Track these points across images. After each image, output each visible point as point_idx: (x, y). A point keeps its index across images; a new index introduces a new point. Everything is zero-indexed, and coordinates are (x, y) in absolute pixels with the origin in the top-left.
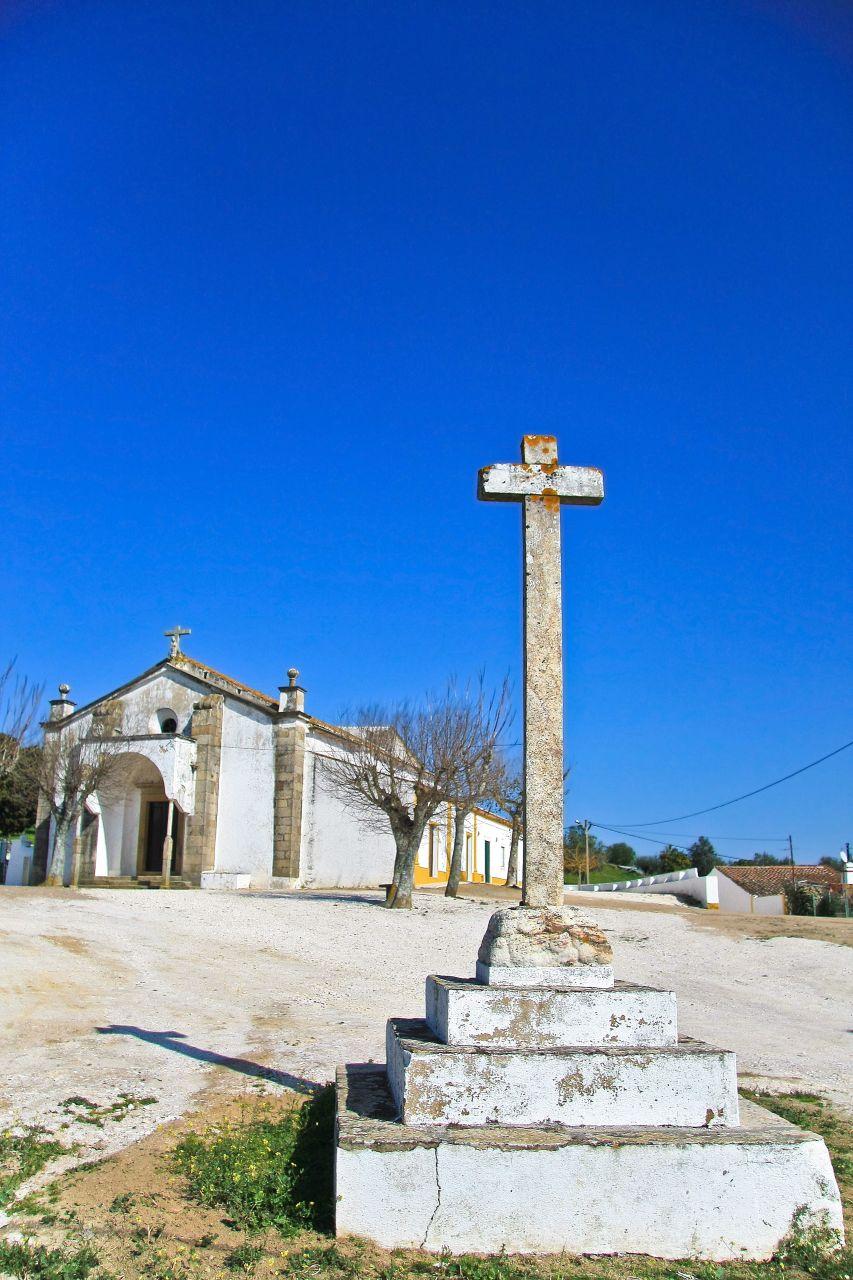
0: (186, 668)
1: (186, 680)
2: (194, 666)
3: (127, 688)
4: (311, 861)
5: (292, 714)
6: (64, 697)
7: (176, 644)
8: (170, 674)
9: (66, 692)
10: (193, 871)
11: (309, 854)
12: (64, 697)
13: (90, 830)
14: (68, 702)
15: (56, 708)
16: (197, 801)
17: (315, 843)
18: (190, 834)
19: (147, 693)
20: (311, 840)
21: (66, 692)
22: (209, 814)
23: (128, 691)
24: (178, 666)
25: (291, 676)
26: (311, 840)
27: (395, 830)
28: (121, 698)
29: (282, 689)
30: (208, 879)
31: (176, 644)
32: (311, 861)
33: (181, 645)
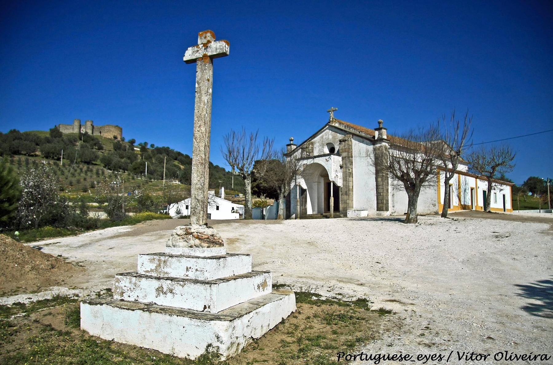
0: (337, 125)
1: (336, 130)
2: (340, 124)
3: (314, 136)
4: (393, 204)
5: (381, 140)
6: (292, 142)
7: (332, 115)
8: (331, 128)
9: (292, 140)
10: (344, 210)
11: (393, 201)
12: (292, 142)
13: (304, 196)
14: (293, 144)
15: (289, 147)
16: (343, 181)
17: (395, 196)
18: (342, 195)
19: (322, 137)
20: (393, 195)
21: (292, 140)
22: (349, 186)
23: (314, 138)
24: (333, 125)
25: (379, 123)
26: (393, 195)
27: (407, 189)
28: (313, 141)
29: (376, 130)
30: (350, 214)
31: (332, 115)
32: (393, 204)
33: (334, 115)
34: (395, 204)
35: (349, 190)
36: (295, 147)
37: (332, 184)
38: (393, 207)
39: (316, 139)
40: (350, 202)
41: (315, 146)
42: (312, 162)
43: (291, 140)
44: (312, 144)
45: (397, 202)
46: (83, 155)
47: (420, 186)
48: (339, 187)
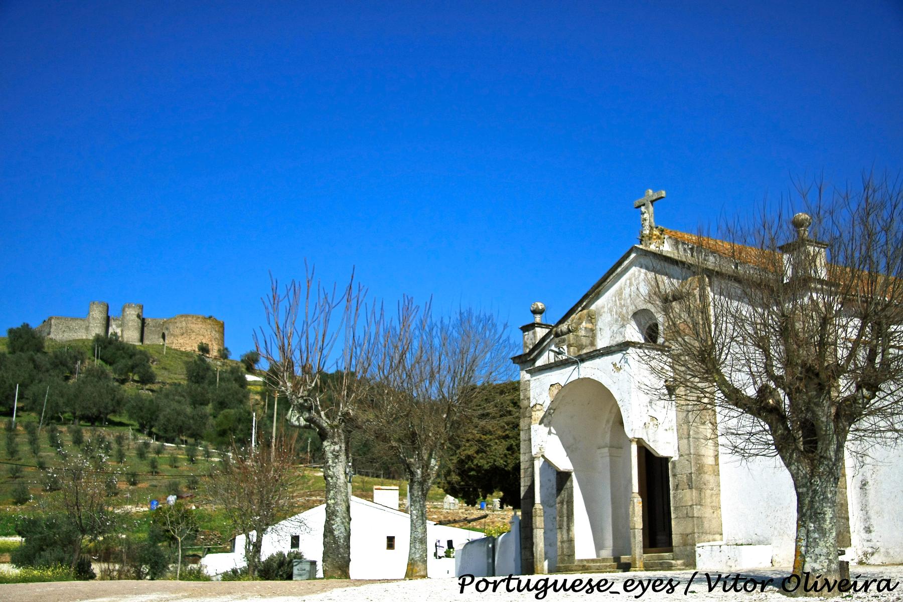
0: (667, 248)
1: (659, 265)
2: (676, 242)
3: (595, 292)
4: (867, 519)
5: (803, 282)
6: (538, 319)
7: (648, 214)
8: (643, 260)
9: (540, 312)
10: (685, 544)
11: (864, 508)
12: (538, 319)
13: (564, 494)
14: (540, 325)
15: (529, 335)
16: (680, 438)
17: (870, 488)
18: (677, 487)
19: (620, 293)
20: (864, 485)
21: (540, 312)
22: (699, 456)
23: (598, 296)
24: (652, 248)
25: (798, 224)
26: (864, 485)
27: (783, 446)
28: (593, 307)
29: (784, 249)
30: (710, 559)
31: (648, 214)
32: (867, 519)
33: (656, 215)
34: (874, 521)
35: (700, 470)
36: (545, 331)
37: (634, 448)
38: (868, 530)
39: (603, 303)
40: (707, 512)
41: (600, 324)
42: (575, 377)
43: (535, 312)
44: (591, 318)
45: (879, 513)
46: (76, 396)
47: (841, 434)
48: (666, 460)
